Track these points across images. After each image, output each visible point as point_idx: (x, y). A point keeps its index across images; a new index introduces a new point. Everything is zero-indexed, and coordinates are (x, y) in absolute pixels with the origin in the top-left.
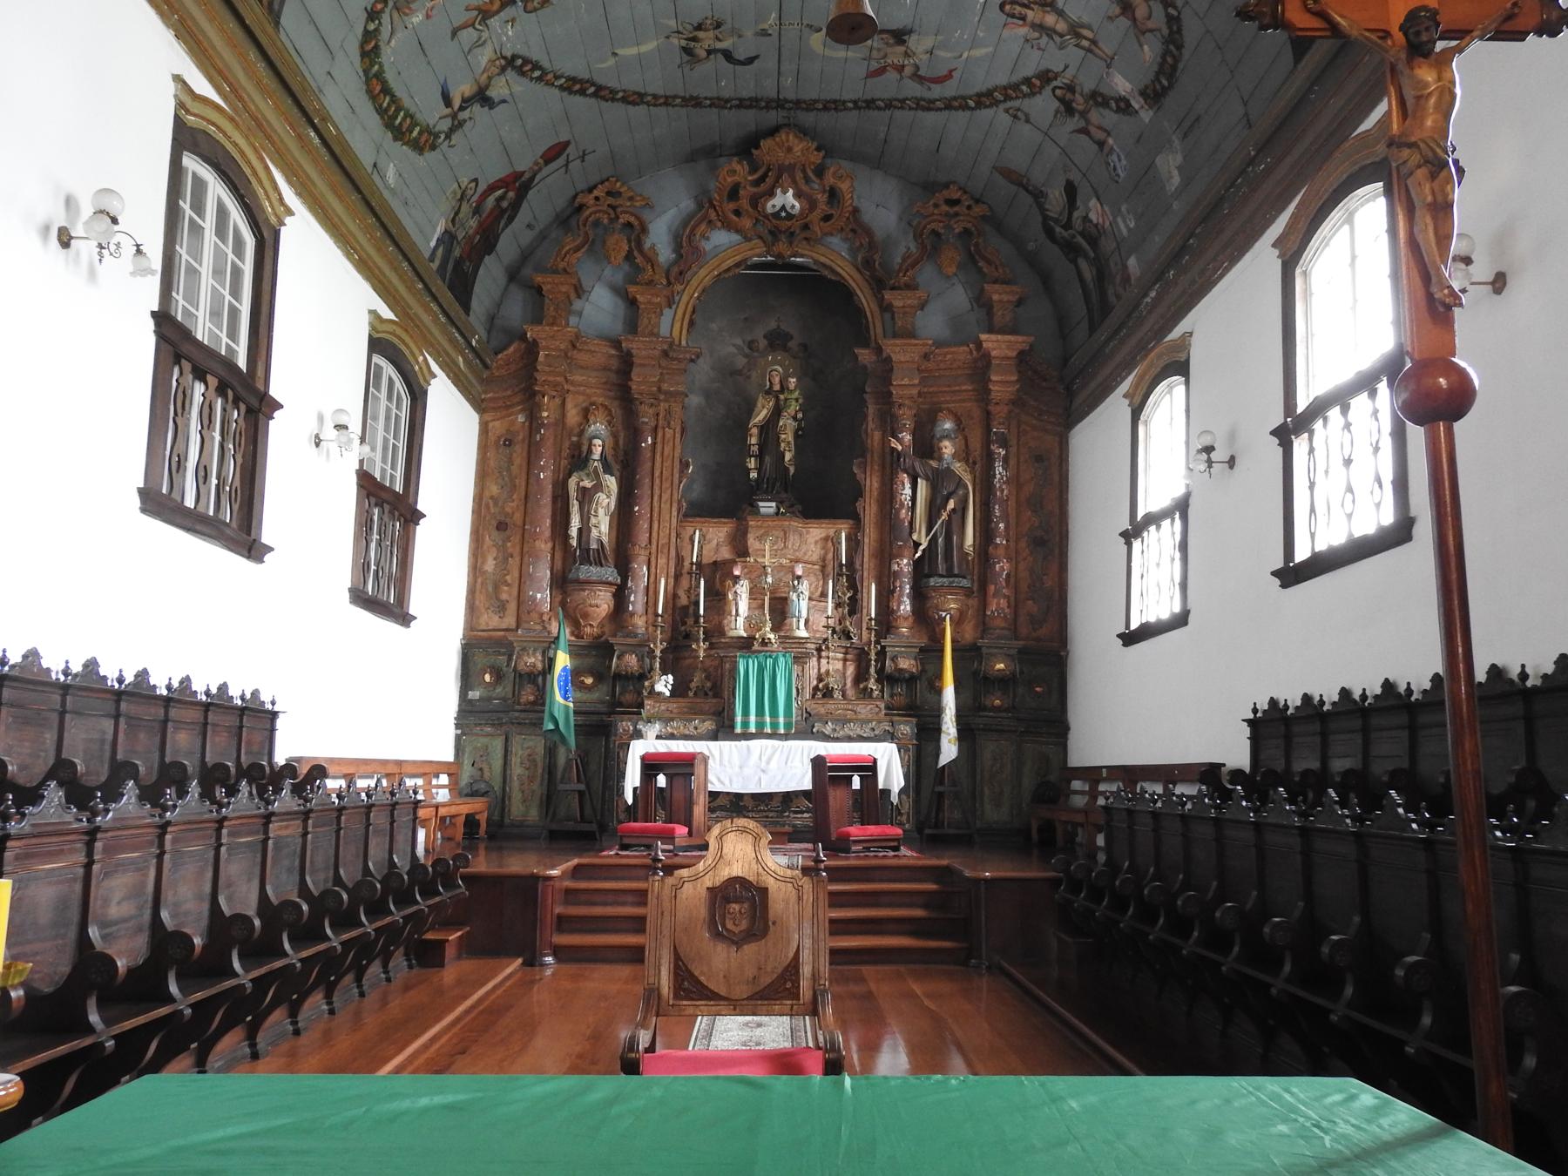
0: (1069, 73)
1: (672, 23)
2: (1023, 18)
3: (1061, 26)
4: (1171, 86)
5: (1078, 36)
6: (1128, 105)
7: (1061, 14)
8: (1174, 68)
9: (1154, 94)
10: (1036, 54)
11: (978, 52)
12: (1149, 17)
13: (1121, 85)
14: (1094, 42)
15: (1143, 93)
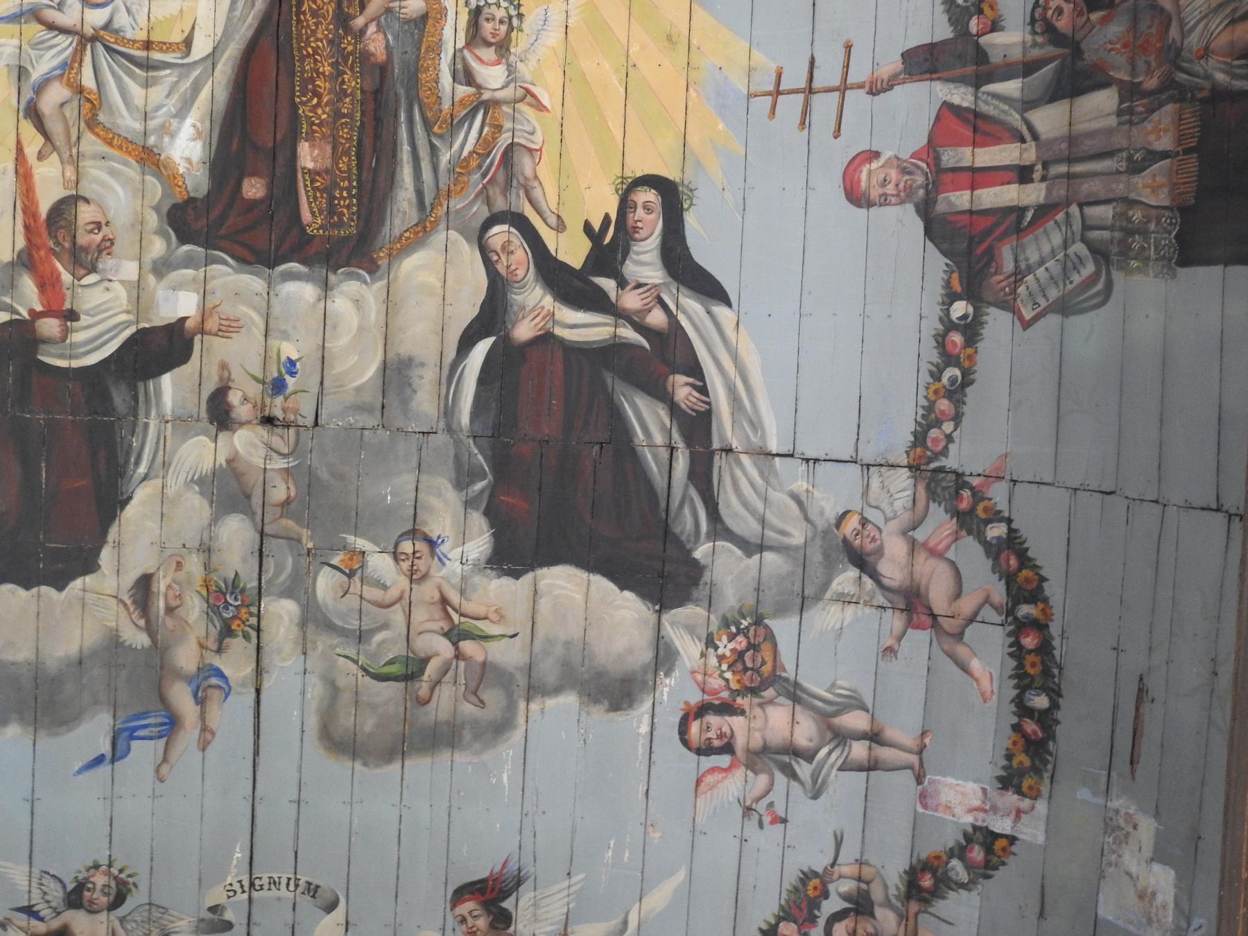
0: (849, 853)
1: (19, 875)
2: (728, 749)
3: (805, 732)
4: (1055, 694)
5: (841, 737)
6: (988, 838)
7: (795, 694)
8: (1045, 648)
9: (1030, 756)
10: (767, 839)
11: (658, 899)
12: (958, 595)
13: (962, 797)
14: (874, 737)
15: (1008, 781)
